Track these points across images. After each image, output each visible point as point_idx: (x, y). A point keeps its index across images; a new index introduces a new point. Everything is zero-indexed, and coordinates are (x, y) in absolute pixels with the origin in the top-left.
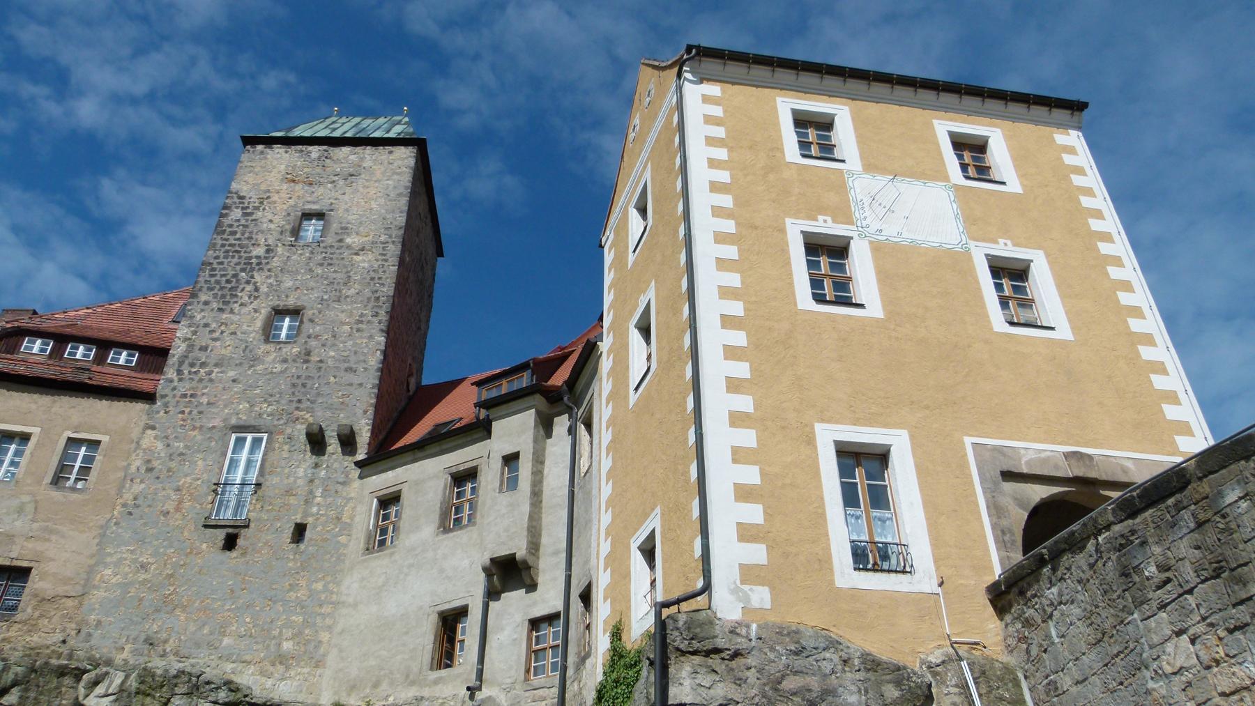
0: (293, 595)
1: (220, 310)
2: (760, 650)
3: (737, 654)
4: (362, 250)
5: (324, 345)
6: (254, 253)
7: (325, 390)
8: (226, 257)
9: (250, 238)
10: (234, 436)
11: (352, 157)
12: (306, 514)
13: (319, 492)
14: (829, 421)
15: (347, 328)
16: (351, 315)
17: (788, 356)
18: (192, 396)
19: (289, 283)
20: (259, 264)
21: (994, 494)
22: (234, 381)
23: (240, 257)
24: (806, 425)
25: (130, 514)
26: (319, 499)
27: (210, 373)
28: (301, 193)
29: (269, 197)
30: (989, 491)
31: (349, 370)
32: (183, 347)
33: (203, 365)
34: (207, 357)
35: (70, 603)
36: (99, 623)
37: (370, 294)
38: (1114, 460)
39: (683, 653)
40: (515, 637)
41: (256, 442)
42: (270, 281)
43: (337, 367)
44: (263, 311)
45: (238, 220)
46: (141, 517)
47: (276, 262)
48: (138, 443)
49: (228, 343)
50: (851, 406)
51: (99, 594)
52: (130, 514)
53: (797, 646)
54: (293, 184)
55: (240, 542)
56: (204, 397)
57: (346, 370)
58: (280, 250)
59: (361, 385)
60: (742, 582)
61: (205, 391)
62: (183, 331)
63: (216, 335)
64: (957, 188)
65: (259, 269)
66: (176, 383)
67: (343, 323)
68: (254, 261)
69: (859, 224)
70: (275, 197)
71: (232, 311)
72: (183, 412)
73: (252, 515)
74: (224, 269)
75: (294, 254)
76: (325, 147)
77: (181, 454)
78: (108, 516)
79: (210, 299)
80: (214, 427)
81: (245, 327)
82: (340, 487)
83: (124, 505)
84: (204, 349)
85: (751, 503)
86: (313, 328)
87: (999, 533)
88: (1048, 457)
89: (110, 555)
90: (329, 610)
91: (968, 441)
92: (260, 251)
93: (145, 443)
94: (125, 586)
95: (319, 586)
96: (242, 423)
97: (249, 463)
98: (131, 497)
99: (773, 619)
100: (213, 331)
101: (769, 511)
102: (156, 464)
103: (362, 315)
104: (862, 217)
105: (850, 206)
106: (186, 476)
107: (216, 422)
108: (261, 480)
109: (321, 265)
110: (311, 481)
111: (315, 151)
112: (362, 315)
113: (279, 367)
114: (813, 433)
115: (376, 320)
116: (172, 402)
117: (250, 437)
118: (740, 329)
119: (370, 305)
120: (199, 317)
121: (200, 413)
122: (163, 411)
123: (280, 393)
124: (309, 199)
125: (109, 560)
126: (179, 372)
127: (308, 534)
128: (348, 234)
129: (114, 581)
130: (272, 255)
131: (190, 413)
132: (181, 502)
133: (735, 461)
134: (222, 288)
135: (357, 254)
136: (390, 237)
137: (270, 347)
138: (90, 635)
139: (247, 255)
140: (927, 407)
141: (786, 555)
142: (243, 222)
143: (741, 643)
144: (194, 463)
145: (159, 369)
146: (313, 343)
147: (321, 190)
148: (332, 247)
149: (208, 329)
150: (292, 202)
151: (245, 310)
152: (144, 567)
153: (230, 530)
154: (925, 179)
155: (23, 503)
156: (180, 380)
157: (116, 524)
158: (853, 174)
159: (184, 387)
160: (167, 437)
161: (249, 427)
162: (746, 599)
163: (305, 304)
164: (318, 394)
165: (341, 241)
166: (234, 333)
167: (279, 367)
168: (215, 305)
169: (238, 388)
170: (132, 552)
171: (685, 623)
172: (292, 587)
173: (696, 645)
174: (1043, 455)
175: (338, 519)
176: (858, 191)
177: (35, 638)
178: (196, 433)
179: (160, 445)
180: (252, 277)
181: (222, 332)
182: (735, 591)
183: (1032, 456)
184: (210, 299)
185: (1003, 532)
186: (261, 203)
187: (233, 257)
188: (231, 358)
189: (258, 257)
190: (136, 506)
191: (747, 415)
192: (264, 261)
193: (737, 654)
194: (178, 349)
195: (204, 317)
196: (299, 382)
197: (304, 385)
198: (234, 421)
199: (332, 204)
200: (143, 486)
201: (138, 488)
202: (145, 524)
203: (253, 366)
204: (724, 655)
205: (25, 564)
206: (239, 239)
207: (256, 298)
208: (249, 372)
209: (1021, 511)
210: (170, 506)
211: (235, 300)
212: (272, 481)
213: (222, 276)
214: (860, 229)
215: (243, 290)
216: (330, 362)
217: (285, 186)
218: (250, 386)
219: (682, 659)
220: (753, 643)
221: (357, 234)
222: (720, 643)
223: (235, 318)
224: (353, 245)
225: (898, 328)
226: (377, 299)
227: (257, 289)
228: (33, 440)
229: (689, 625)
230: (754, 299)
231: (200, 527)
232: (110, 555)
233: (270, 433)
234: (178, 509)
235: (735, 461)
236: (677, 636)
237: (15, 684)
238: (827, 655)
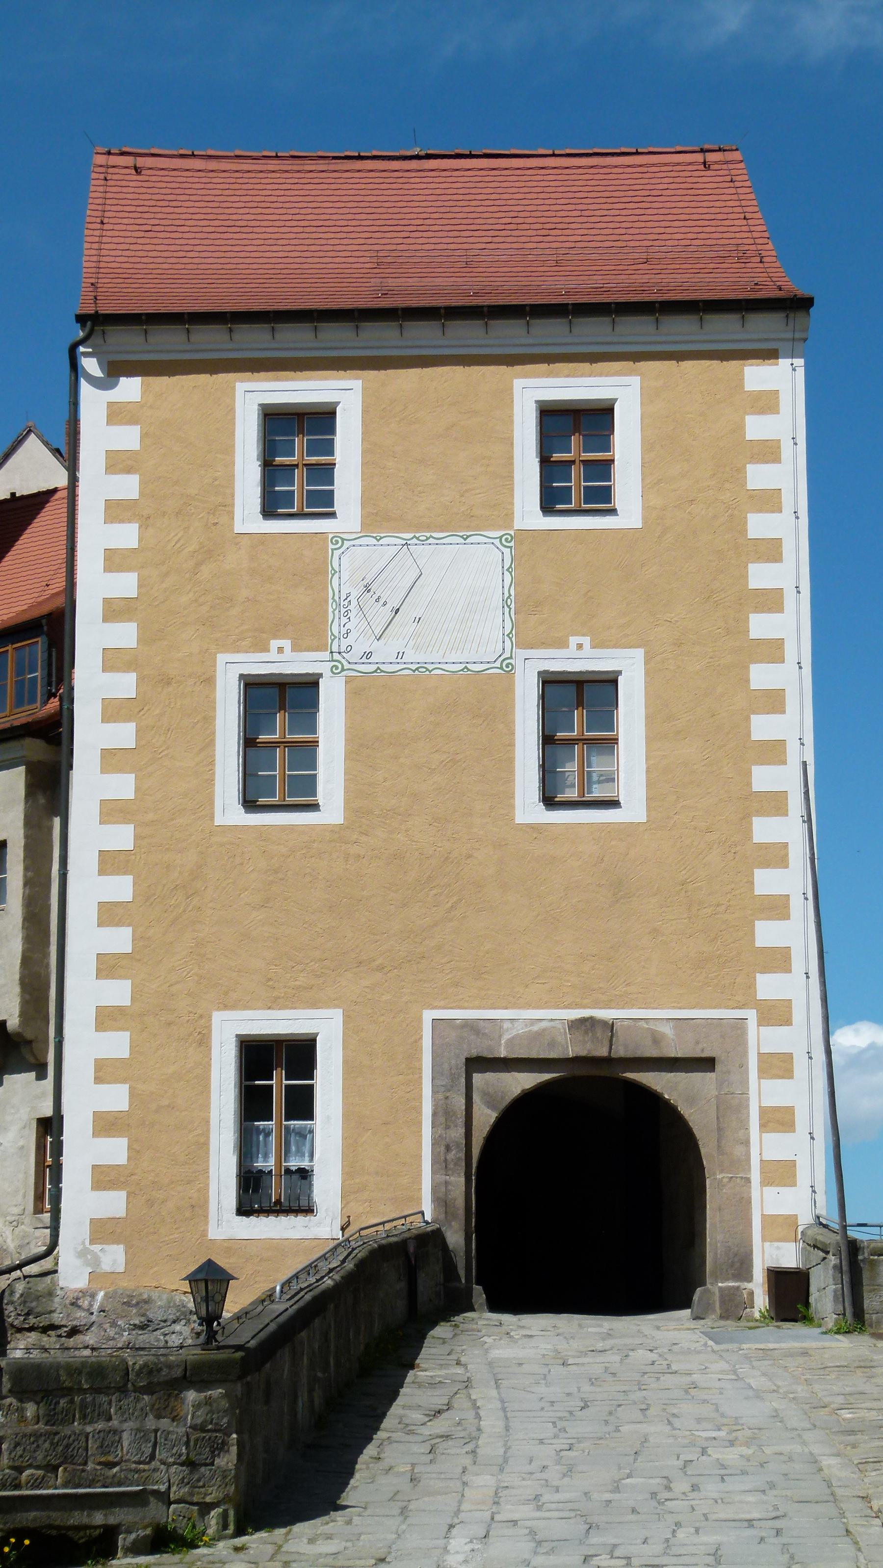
2: (100, 1325)
3: (74, 1331)
14: (233, 1007)
17: (190, 908)
21: (448, 1094)
24: (201, 1016)
30: (443, 1089)
38: (645, 1026)
39: (20, 1330)
40: (21, 1143)
50: (270, 980)
53: (143, 1319)
60: (92, 1242)
64: (524, 537)
69: (335, 648)
85: (114, 1137)
87: (443, 1148)
88: (544, 1030)
91: (429, 1015)
99: (125, 1284)
101: (135, 1146)
104: (343, 631)
105: (327, 611)
114: (209, 1027)
118: (125, 873)
133: (98, 1080)
140: (380, 968)
141: (150, 1203)
143: (80, 1317)
154: (468, 528)
158: (343, 540)
162: (97, 1261)
171: (22, 1295)
173: (32, 1320)
174: (535, 1028)
176: (345, 576)
182: (82, 1254)
183: (520, 1029)
185: (448, 1148)
191: (121, 1010)
193: (74, 1331)
204: (59, 1332)
209: (489, 1111)
214: (336, 656)
219: (18, 1335)
220: (94, 1318)
222: (57, 1318)
225: (364, 838)
229: (26, 1297)
230: (150, 816)
235: (98, 1080)
236: (11, 1312)
238: (177, 1327)
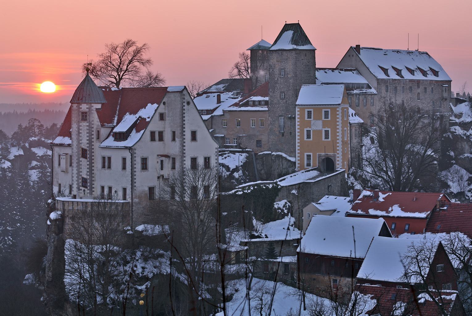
0: (291, 143)
6: (275, 80)
8: (272, 81)
10: (280, 117)
11: (286, 54)
12: (291, 131)
13: (292, 127)
16: (291, 93)
27: (275, 106)
33: (273, 104)
36: (271, 147)
42: (279, 86)
67: (290, 95)
70: (276, 66)
76: (281, 51)
92: (276, 79)
94: (273, 142)
100: (273, 97)
102: (271, 122)
103: (293, 93)
111: (280, 52)
113: (284, 104)
115: (295, 94)
117: (282, 117)
126: (271, 106)
128: (288, 75)
135: (290, 79)
137: (281, 100)
138: (270, 149)
146: (287, 99)
151: (277, 92)
164: (289, 109)
165: (287, 76)
167: (283, 104)
169: (279, 108)
172: (291, 142)
178: (275, 117)
189: (276, 81)
190: (271, 130)
196: (286, 107)
198: (279, 115)
216: (290, 103)
227: (277, 88)
228: (256, 120)
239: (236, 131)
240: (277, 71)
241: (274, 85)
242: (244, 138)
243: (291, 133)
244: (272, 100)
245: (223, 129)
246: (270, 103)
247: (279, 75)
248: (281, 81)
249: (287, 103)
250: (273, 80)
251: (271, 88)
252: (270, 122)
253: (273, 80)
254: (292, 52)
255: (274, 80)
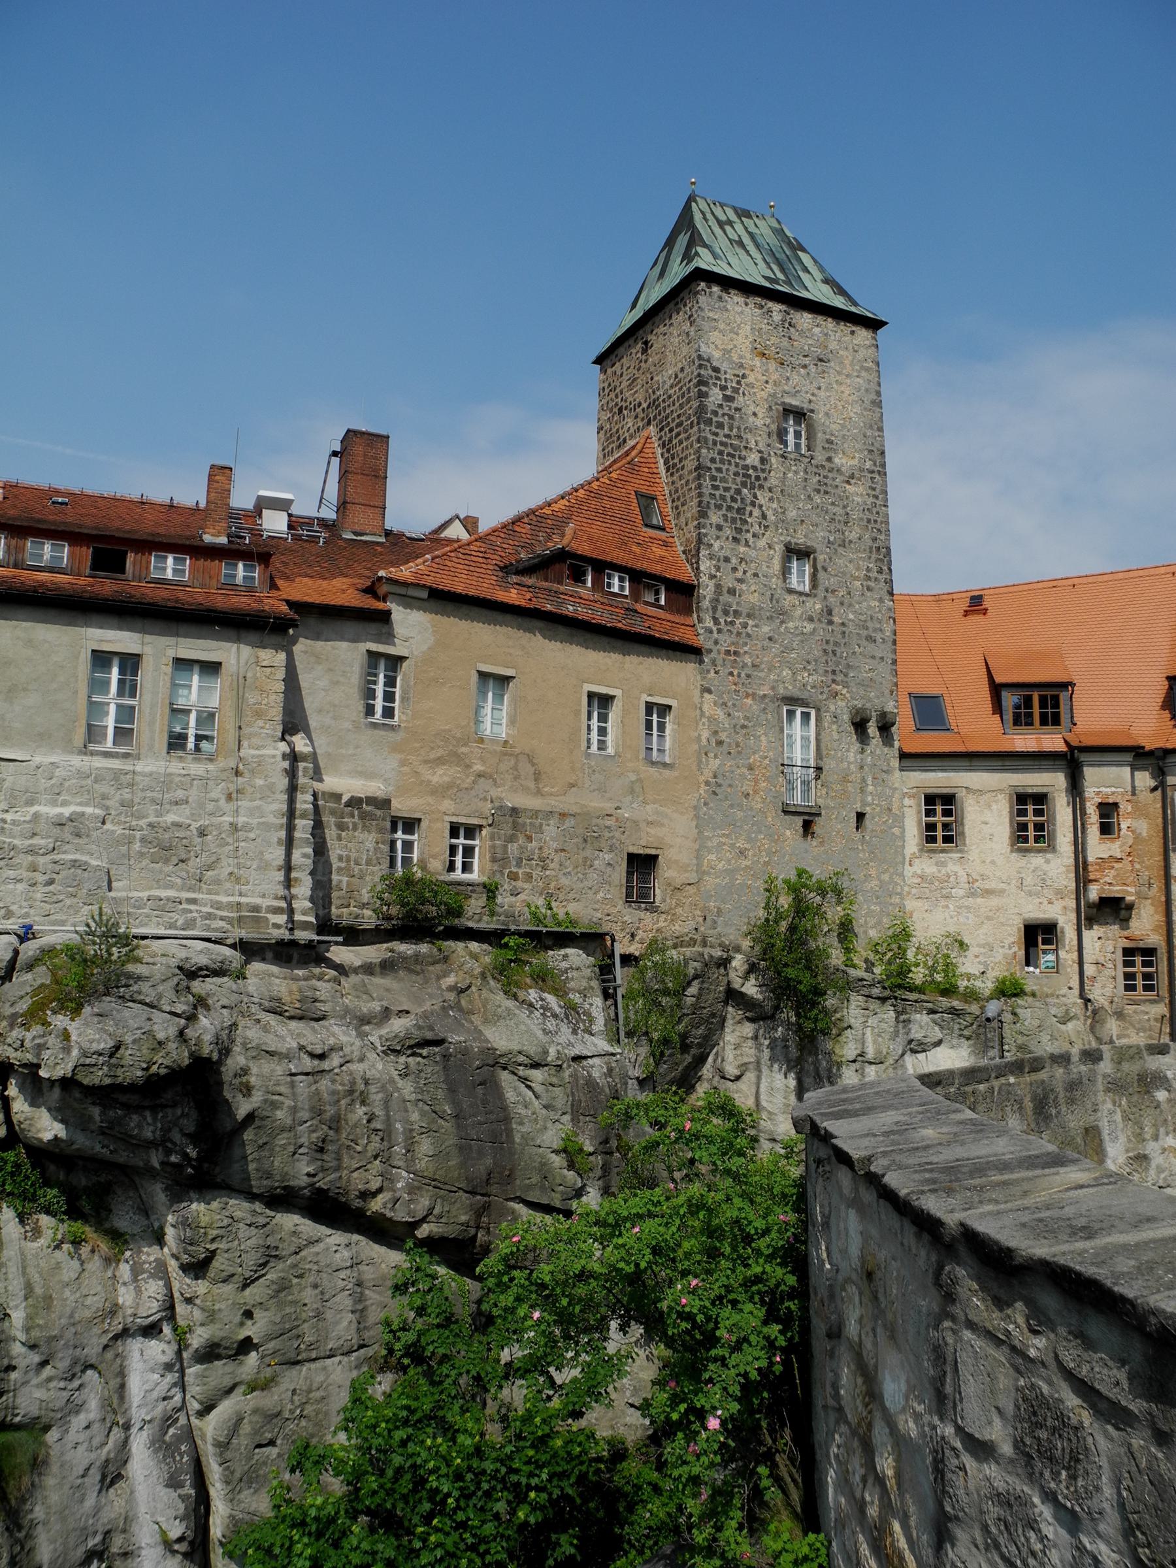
1: (735, 540)
4: (852, 476)
5: (842, 604)
6: (748, 462)
7: (853, 661)
8: (722, 461)
9: (739, 437)
11: (816, 330)
13: (870, 782)
15: (858, 583)
18: (735, 653)
19: (792, 514)
20: (758, 478)
22: (770, 639)
23: (737, 465)
25: (715, 793)
26: (871, 788)
27: (745, 626)
28: (775, 376)
29: (744, 376)
31: (871, 639)
32: (711, 583)
34: (738, 603)
35: (691, 890)
36: (719, 911)
37: (870, 543)
41: (805, 716)
43: (858, 634)
44: (777, 547)
45: (721, 406)
46: (726, 798)
47: (773, 481)
48: (701, 709)
49: (753, 588)
51: (710, 882)
52: (715, 793)
54: (764, 360)
55: (816, 828)
56: (747, 656)
57: (867, 639)
58: (773, 460)
59: (882, 658)
61: (746, 649)
62: (705, 565)
63: (739, 574)
65: (761, 487)
66: (715, 635)
67: (857, 578)
68: (751, 472)
70: (751, 379)
71: (747, 544)
72: (731, 674)
73: (821, 802)
74: (723, 480)
75: (789, 470)
77: (744, 727)
78: (697, 795)
79: (721, 521)
80: (765, 695)
81: (764, 568)
82: (885, 776)
83: (707, 783)
84: (731, 592)
86: (829, 579)
89: (709, 838)
90: (897, 901)
92: (753, 459)
93: (706, 707)
94: (731, 872)
95: (886, 877)
96: (789, 694)
97: (805, 739)
98: (711, 775)
100: (735, 569)
102: (723, 736)
106: (754, 753)
107: (765, 690)
108: (821, 764)
109: (818, 491)
110: (862, 767)
112: (868, 570)
116: (719, 662)
119: (873, 559)
120: (717, 545)
121: (748, 676)
122: (712, 672)
123: (816, 661)
124: (786, 388)
125: (709, 844)
126: (716, 621)
127: (867, 822)
129: (720, 866)
130: (768, 467)
131: (739, 675)
132: (756, 782)
134: (729, 508)
135: (848, 482)
136: (875, 464)
138: (714, 924)
139: (742, 463)
142: (726, 410)
144: (757, 738)
145: (687, 610)
146: (832, 600)
147: (795, 378)
148: (823, 467)
149: (730, 566)
150: (770, 388)
151: (762, 543)
152: (742, 852)
153: (806, 818)
155: (632, 782)
156: (719, 631)
157: (705, 804)
159: (726, 641)
160: (725, 704)
161: (798, 699)
163: (815, 545)
165: (829, 459)
166: (756, 575)
167: (809, 627)
168: (728, 532)
169: (776, 648)
170: (727, 836)
175: (890, 810)
177: (677, 927)
178: (749, 701)
179: (720, 713)
180: (755, 496)
181: (745, 572)
184: (721, 521)
186: (739, 383)
187: (730, 463)
188: (761, 609)
189: (755, 468)
192: (763, 475)
194: (707, 591)
195: (722, 548)
196: (830, 648)
197: (834, 653)
199: (810, 401)
200: (718, 762)
201: (714, 764)
202: (732, 806)
203: (782, 622)
205: (653, 852)
206: (728, 436)
207: (766, 527)
208: (782, 630)
210: (748, 787)
211: (745, 528)
212: (829, 765)
213: (727, 489)
215: (751, 514)
216: (851, 628)
217: (757, 362)
218: (786, 648)
221: (844, 453)
223: (753, 553)
224: (843, 469)
226: (878, 549)
227: (764, 516)
231: (780, 812)
232: (709, 838)
233: (818, 710)
234: (756, 792)
237: (696, 977)
239: (478, 767)
240: (761, 412)
241: (738, 492)
242: (551, 830)
243: (860, 816)
244: (729, 582)
245: (377, 732)
246: (706, 603)
247: (775, 437)
248: (790, 475)
249: (830, 623)
250: (733, 456)
251: (719, 507)
252: (716, 733)
253: (729, 454)
254: (853, 333)
255: (744, 459)
